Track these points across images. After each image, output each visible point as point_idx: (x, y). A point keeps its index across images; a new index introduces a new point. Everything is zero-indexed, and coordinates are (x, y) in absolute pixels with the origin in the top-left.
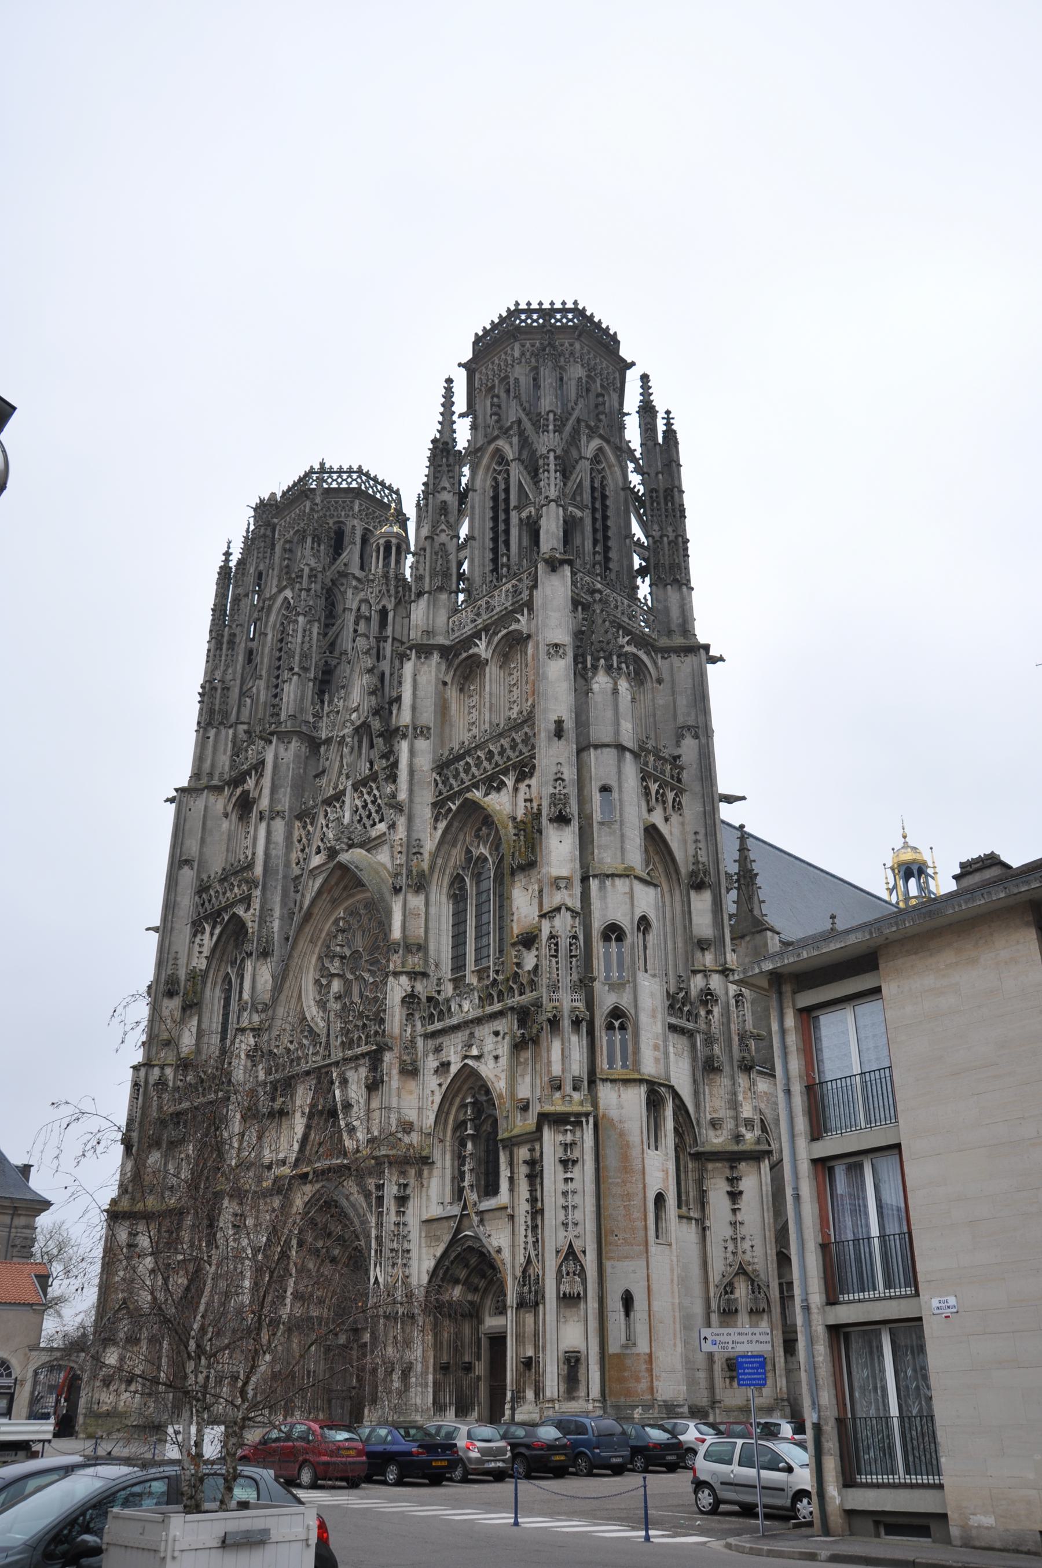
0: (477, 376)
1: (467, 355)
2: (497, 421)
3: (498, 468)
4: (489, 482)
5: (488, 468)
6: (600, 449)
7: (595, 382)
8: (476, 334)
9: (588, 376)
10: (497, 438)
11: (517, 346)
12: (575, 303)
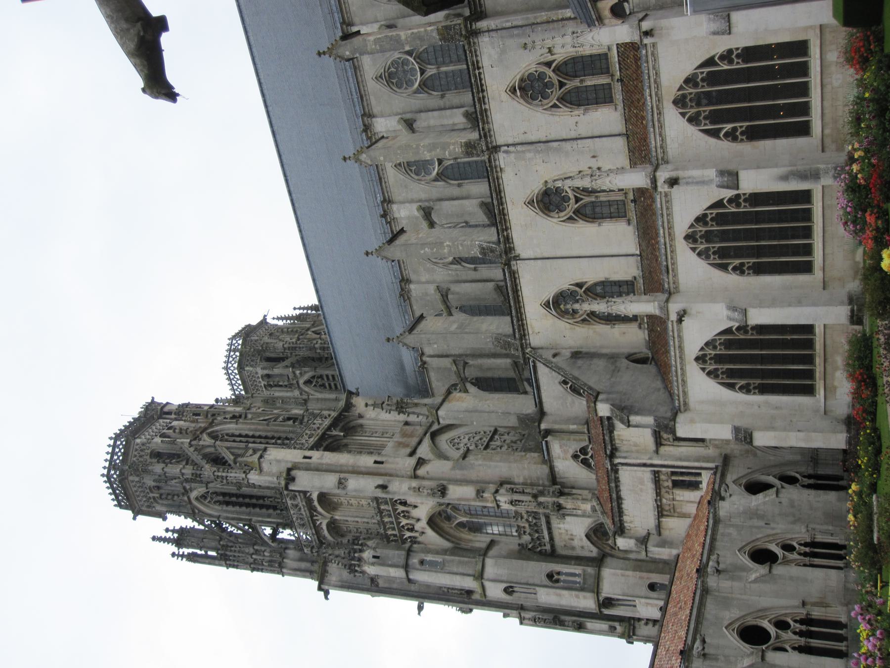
0: (144, 508)
1: (129, 513)
2: (178, 496)
4: (216, 507)
5: (207, 506)
6: (209, 435)
7: (164, 433)
8: (115, 505)
9: (160, 436)
10: (189, 498)
11: (131, 478)
12: (111, 438)
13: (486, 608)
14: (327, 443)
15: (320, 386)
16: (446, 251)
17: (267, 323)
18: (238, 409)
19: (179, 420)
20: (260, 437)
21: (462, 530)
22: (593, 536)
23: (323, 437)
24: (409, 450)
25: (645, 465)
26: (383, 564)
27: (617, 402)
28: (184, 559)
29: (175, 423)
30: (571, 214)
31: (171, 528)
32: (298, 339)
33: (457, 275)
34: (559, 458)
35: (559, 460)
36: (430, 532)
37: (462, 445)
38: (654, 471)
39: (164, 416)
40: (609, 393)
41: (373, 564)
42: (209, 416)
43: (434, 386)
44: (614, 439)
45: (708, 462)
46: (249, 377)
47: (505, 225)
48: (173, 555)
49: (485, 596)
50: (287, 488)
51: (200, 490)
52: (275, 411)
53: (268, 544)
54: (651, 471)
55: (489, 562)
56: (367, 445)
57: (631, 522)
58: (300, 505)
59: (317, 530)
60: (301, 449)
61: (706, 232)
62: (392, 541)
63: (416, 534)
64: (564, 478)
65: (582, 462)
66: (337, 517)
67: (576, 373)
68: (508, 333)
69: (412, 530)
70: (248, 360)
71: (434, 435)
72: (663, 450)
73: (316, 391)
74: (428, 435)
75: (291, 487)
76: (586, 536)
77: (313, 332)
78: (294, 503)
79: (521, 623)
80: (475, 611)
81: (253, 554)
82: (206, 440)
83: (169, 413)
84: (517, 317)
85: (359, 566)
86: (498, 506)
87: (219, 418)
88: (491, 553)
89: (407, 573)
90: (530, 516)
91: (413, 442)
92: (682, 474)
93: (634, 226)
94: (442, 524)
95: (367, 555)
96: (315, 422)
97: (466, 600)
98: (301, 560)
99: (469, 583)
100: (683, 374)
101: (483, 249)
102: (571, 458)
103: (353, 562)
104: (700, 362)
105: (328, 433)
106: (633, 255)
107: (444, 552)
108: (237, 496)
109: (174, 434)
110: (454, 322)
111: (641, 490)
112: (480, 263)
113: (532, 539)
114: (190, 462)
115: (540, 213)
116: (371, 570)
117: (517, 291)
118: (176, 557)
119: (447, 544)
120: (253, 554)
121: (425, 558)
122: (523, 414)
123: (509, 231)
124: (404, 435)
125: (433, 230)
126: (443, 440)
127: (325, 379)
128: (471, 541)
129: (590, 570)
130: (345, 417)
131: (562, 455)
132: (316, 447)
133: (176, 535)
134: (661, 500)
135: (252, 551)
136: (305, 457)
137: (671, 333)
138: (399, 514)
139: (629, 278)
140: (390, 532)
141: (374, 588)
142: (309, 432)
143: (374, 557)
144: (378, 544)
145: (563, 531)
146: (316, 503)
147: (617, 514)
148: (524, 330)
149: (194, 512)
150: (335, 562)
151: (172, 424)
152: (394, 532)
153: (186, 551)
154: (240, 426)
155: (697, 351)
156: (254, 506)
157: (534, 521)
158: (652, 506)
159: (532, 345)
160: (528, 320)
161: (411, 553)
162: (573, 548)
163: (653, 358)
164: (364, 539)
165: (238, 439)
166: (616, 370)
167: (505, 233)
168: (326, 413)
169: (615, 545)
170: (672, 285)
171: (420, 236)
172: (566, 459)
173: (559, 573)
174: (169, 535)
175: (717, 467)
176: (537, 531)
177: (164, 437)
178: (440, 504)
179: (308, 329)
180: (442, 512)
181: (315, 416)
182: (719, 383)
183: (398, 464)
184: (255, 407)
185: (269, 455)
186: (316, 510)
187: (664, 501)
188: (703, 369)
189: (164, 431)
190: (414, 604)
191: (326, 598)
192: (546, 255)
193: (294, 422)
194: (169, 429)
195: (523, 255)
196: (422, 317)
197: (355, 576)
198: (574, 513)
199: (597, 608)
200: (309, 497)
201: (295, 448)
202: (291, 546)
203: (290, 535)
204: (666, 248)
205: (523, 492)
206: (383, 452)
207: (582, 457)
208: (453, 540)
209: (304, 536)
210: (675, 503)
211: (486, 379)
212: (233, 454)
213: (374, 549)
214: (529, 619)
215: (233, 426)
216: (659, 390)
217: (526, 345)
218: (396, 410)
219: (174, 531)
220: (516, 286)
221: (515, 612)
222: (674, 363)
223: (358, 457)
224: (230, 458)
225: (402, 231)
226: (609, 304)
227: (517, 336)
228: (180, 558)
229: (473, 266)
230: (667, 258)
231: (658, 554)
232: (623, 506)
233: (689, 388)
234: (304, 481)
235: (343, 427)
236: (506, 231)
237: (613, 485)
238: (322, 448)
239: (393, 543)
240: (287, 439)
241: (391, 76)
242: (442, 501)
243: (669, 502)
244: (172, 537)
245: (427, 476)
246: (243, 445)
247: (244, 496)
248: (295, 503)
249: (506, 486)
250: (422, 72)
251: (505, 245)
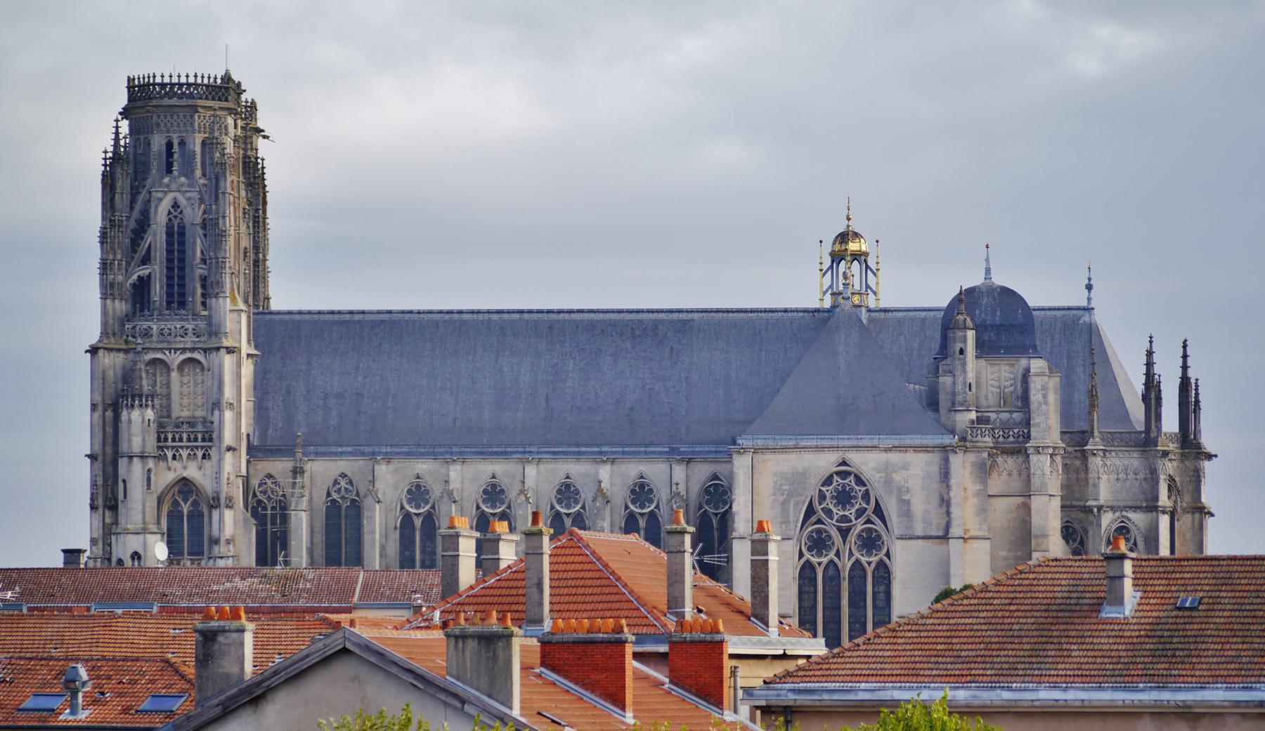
36: (170, 477)
43: (277, 463)
69: (174, 458)
112: (401, 532)
135: (119, 256)
146: (188, 355)
186: (181, 353)
229: (398, 525)
234: (228, 361)
241: (568, 486)
250: (568, 515)
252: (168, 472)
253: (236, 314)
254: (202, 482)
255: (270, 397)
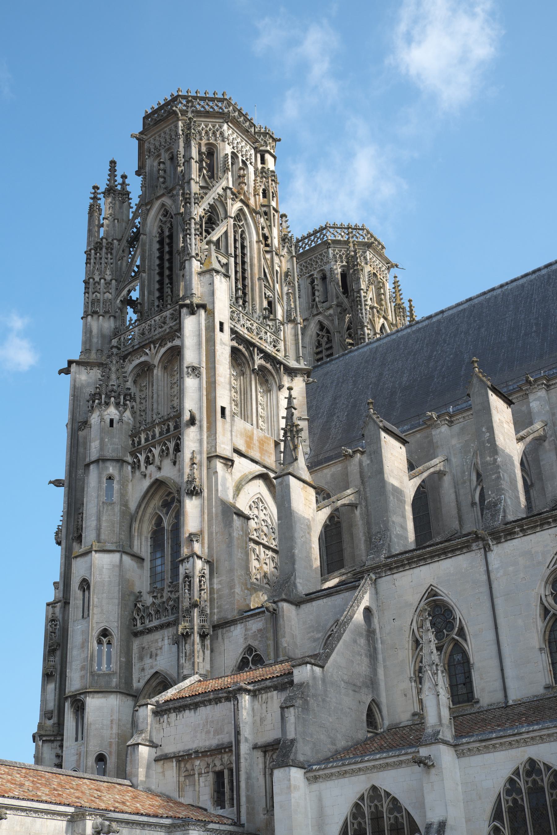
0: (146, 145)
2: (164, 183)
3: (164, 219)
6: (241, 210)
7: (237, 157)
9: (233, 153)
10: (163, 195)
13: (63, 560)
14: (244, 350)
15: (319, 342)
16: (488, 458)
17: (388, 269)
18: (276, 242)
19: (255, 174)
20: (244, 271)
21: (153, 522)
22: (158, 681)
23: (249, 344)
24: (242, 448)
25: (237, 733)
26: (102, 430)
27: (312, 691)
28: (92, 201)
29: (251, 169)
30: (552, 611)
31: (127, 181)
32: (372, 308)
33: (464, 482)
34: (246, 630)
35: (243, 629)
36: (146, 483)
37: (256, 512)
38: (232, 746)
39: (259, 156)
40: (324, 680)
41: (102, 420)
42: (264, 209)
43: (326, 471)
44: (266, 692)
45: (248, 813)
46: (321, 255)
47: (528, 529)
48: (96, 188)
49: (76, 557)
50: (182, 306)
51: (173, 207)
52: (277, 286)
53: (118, 296)
54: (232, 743)
55: (117, 556)
56: (245, 399)
57: (169, 723)
58: (166, 327)
59: (140, 349)
60: (232, 318)
61: (543, 788)
62: (133, 440)
63: (143, 468)
64: (223, 639)
65: (243, 658)
66: (155, 372)
67: (346, 637)
68: (393, 550)
69: (148, 462)
70: (340, 251)
71: (263, 477)
72: (259, 754)
73: (311, 336)
74: (265, 470)
75: (184, 311)
76: (157, 673)
77: (383, 324)
78: (168, 319)
79: (48, 605)
80: (60, 547)
81: (105, 280)
82: (234, 208)
83: (263, 161)
84: (412, 558)
85: (100, 404)
86: (182, 561)
87: (262, 220)
88: (127, 559)
89: (97, 461)
90: (175, 601)
91: (256, 455)
92: (231, 782)
93: (545, 694)
94: (157, 497)
95: (112, 412)
96: (269, 334)
97: (71, 536)
98: (103, 336)
99: (89, 536)
100: (353, 772)
101: (496, 505)
102: (247, 644)
103: (103, 396)
104: (371, 793)
105: (256, 349)
106: (506, 696)
107: (125, 504)
108: (171, 253)
109: (237, 169)
110: (401, 482)
111: (208, 732)
113: (148, 607)
114: (205, 191)
115: (549, 572)
116: (94, 419)
117: (445, 553)
118: (93, 191)
119: (133, 506)
120: (105, 280)
121: (115, 482)
122: (295, 579)
123: (521, 534)
124: (262, 442)
125: (515, 441)
126: (260, 487)
127: (328, 346)
128: (140, 534)
129: (115, 681)
130: (277, 371)
131: (250, 633)
132: (236, 335)
133: (119, 187)
134: (197, 758)
135: (108, 278)
136: (221, 324)
137: (403, 752)
138: (165, 444)
139: (477, 694)
140: (143, 436)
141: (76, 426)
142: (254, 328)
143: (112, 421)
144: (128, 424)
145: (160, 644)
146: (169, 345)
147: (177, 705)
148: (397, 567)
149: (146, 204)
150: (102, 376)
151: (249, 166)
152: (143, 441)
153: (102, 202)
154: (255, 246)
155: (384, 788)
156: (161, 274)
157: (169, 608)
158: (190, 747)
159: (379, 580)
160: (411, 571)
161: (118, 465)
162: (141, 658)
163: (377, 734)
164: (132, 407)
165: (239, 245)
166: (356, 689)
167: (517, 529)
168: (281, 346)
169: (140, 706)
170: (466, 747)
171: (505, 425)
172: (245, 639)
173: (109, 643)
174: (119, 180)
175: (243, 826)
176: (157, 612)
177: (232, 157)
178: (179, 491)
179: (386, 319)
180: (171, 496)
181: (276, 332)
182: (346, 822)
183: (224, 435)
184: (281, 261)
185: (221, 281)
186: (161, 346)
187: (197, 762)
188: (362, 798)
189: (240, 158)
190: (62, 475)
191: (60, 372)
192: (495, 585)
193: (265, 309)
194: (243, 161)
195: (492, 556)
196: (404, 442)
197: (88, 401)
198: (181, 655)
199: (71, 694)
200: (176, 336)
201: (233, 312)
202: (118, 323)
203: (131, 320)
204: (514, 735)
205: (201, 590)
206: (237, 419)
207: (250, 659)
208: (140, 513)
209: (131, 337)
210: (196, 776)
211: (339, 534)
212: (218, 240)
213: (121, 420)
214: (54, 613)
215: (255, 238)
216: (333, 744)
217: (379, 573)
218: (286, 425)
219: (123, 184)
220: (453, 551)
221: (61, 595)
222: (366, 759)
223: (228, 387)
224: (215, 236)
225: (509, 403)
226: (434, 667)
227: (389, 560)
228: (92, 196)
230: (501, 737)
231: (131, 761)
232: (187, 711)
233: (336, 781)
235: (266, 368)
236: (521, 531)
237: (212, 696)
238: (236, 345)
239: (131, 442)
240: (245, 302)
242: (183, 492)
243: (196, 769)
244: (116, 183)
245: (211, 472)
246: (231, 250)
247: (171, 261)
248: (168, 321)
249: (207, 567)
251: (502, 531)
252: (144, 481)
253: (208, 276)
254: (177, 480)
255: (334, 418)
